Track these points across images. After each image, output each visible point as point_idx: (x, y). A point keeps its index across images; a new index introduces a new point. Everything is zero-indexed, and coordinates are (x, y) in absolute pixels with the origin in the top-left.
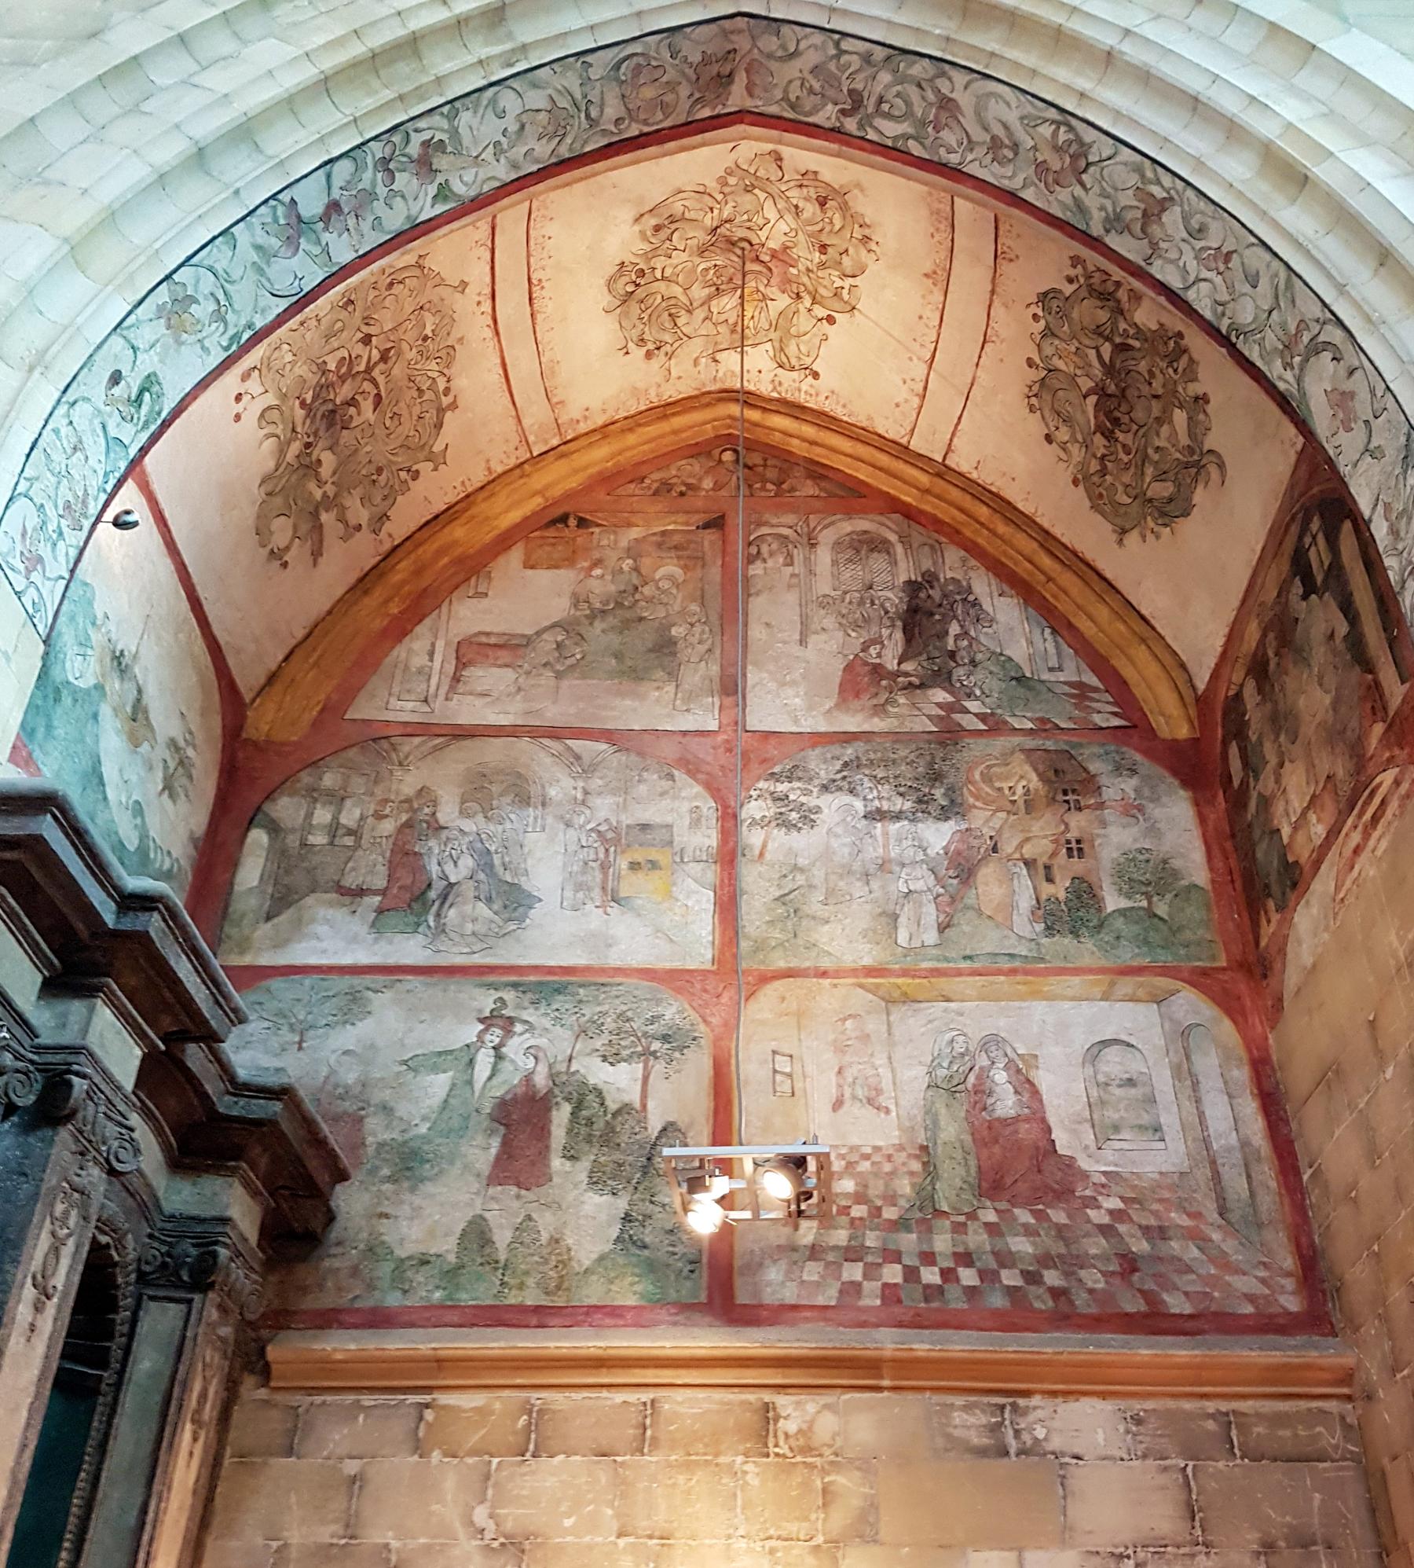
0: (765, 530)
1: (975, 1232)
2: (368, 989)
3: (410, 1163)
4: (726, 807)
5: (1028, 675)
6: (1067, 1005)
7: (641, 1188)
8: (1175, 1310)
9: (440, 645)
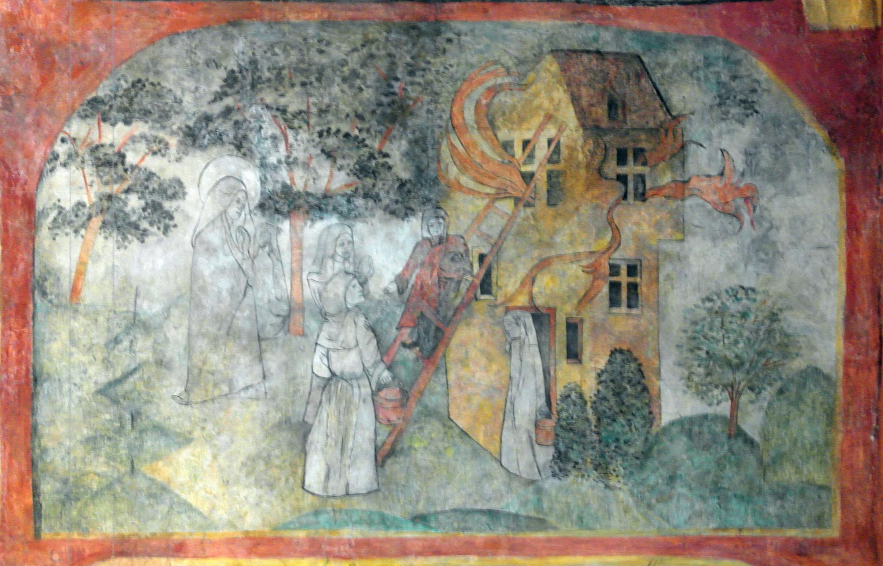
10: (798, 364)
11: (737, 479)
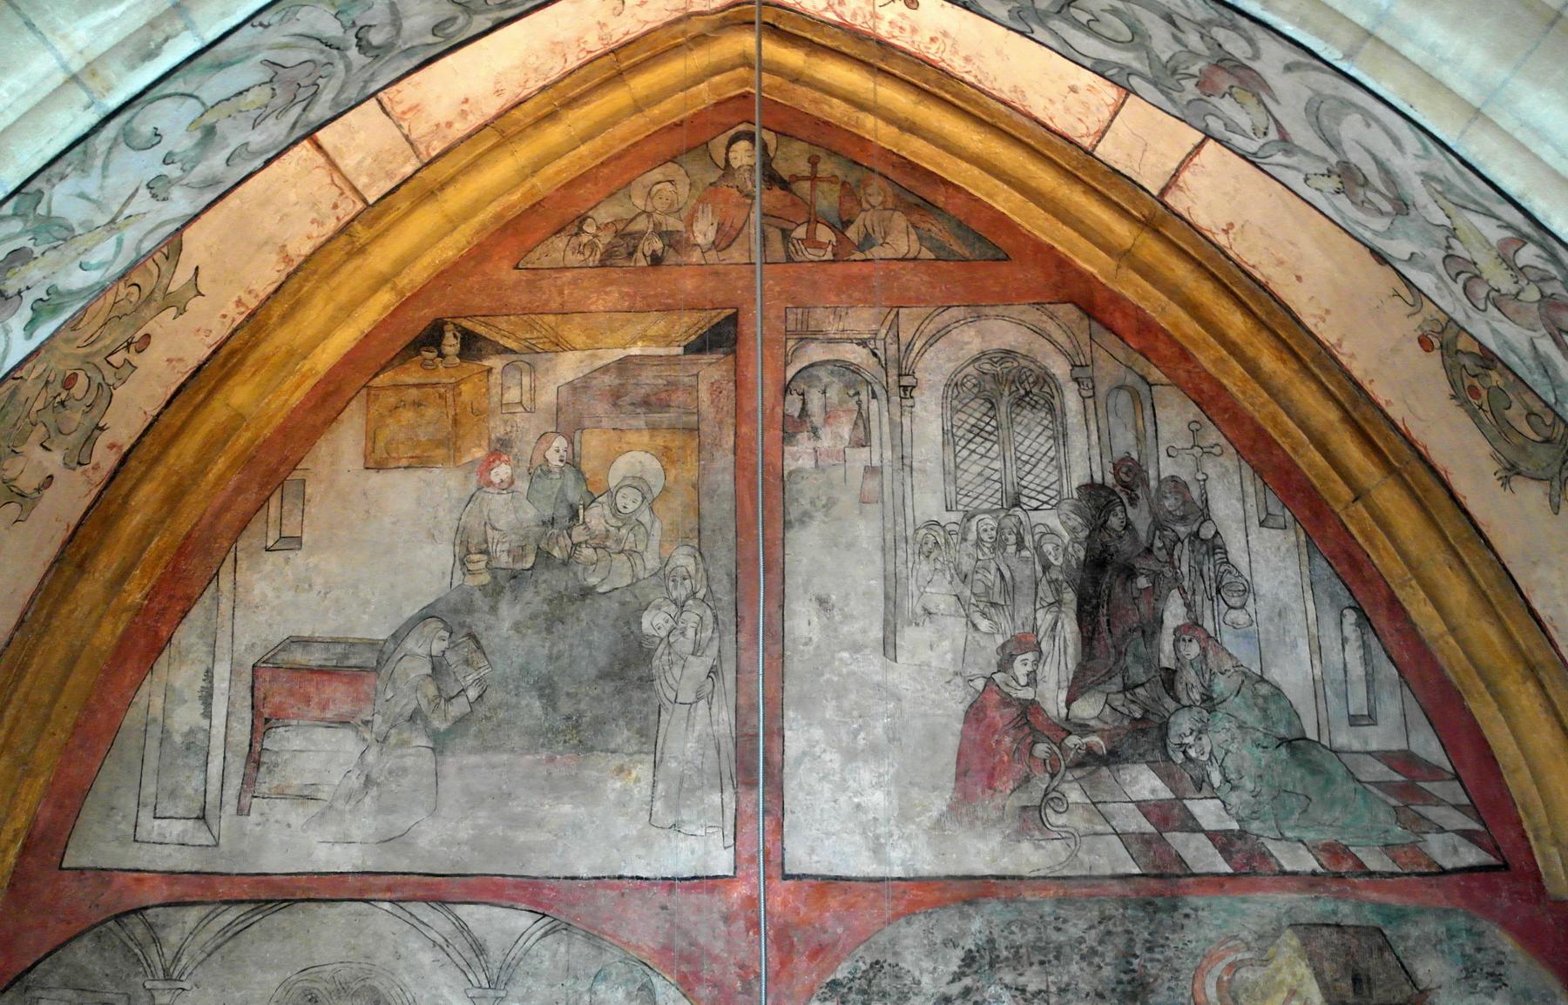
5: (1311, 734)
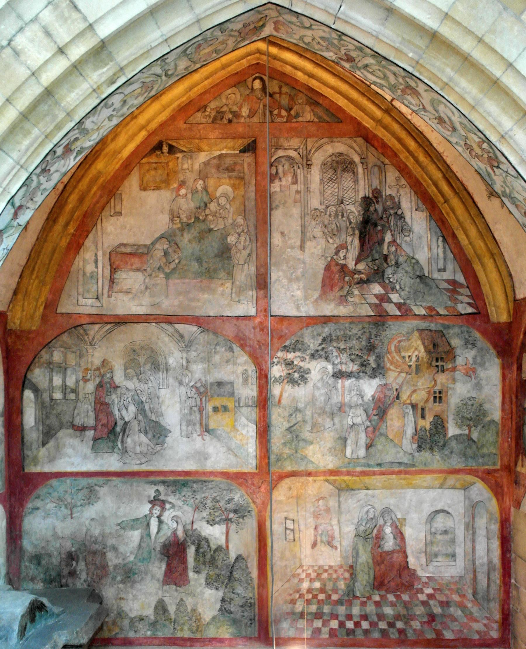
0: (280, 153)
1: (370, 606)
2: (96, 485)
3: (129, 575)
4: (261, 370)
5: (427, 274)
6: (422, 491)
7: (228, 587)
8: (447, 638)
9: (100, 254)
10: (488, 419)
11: (470, 452)
